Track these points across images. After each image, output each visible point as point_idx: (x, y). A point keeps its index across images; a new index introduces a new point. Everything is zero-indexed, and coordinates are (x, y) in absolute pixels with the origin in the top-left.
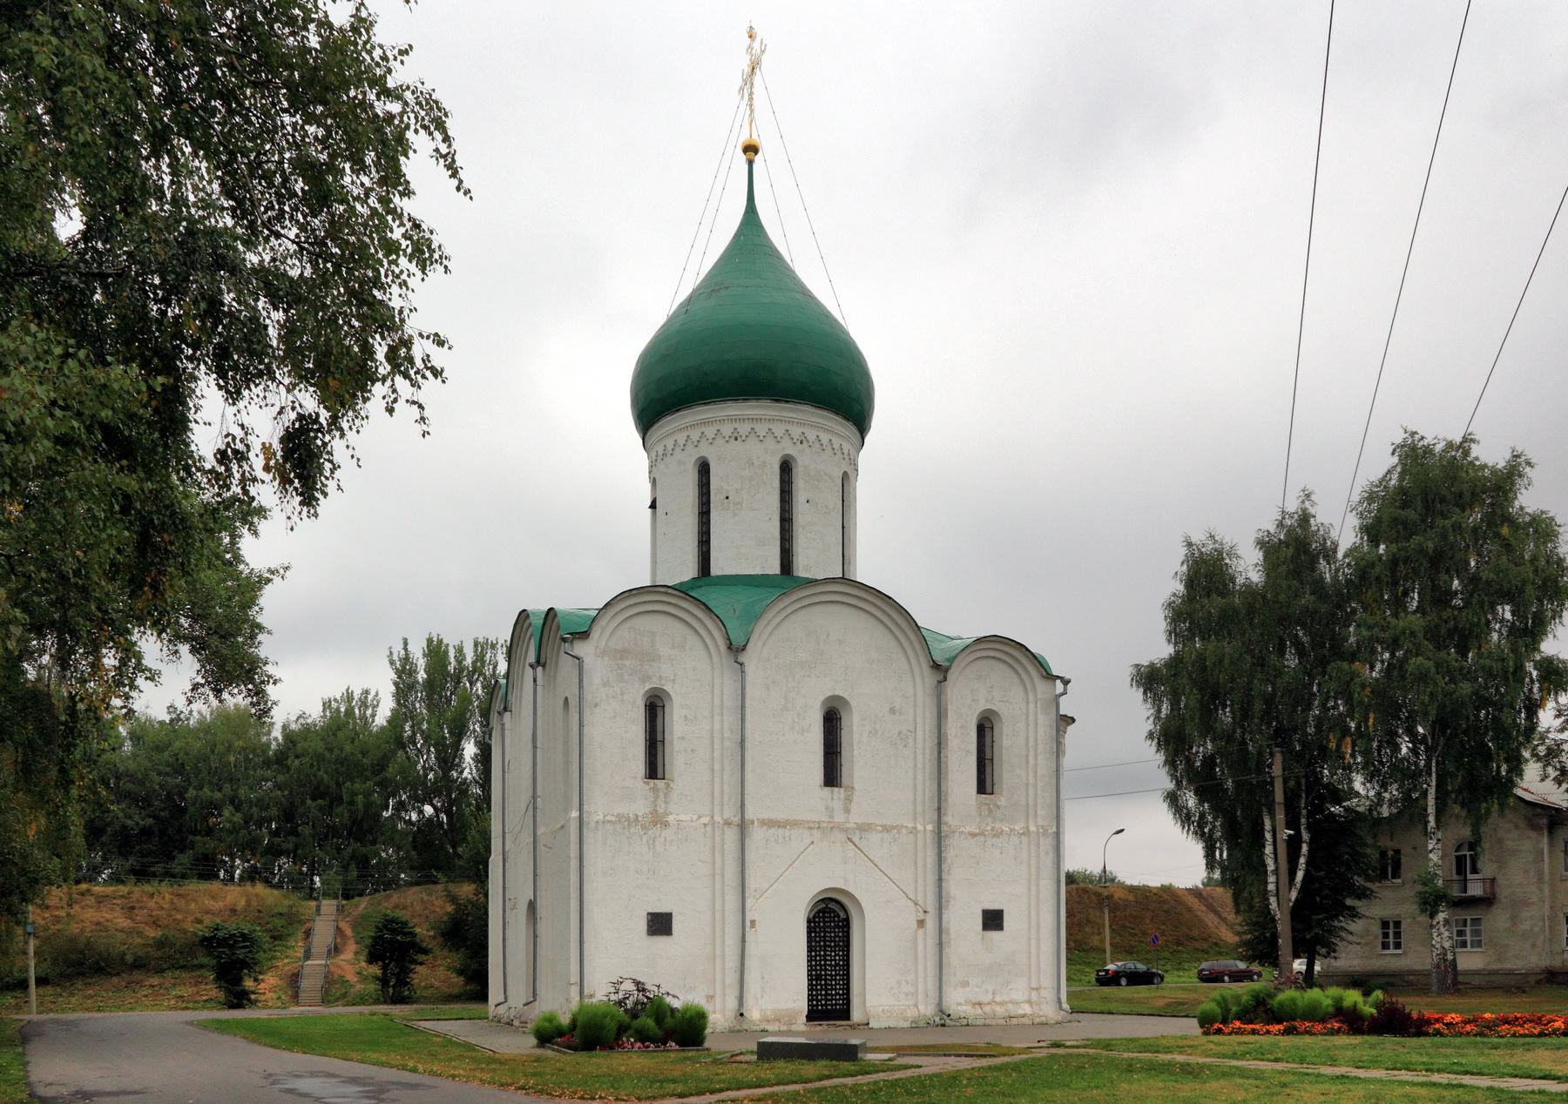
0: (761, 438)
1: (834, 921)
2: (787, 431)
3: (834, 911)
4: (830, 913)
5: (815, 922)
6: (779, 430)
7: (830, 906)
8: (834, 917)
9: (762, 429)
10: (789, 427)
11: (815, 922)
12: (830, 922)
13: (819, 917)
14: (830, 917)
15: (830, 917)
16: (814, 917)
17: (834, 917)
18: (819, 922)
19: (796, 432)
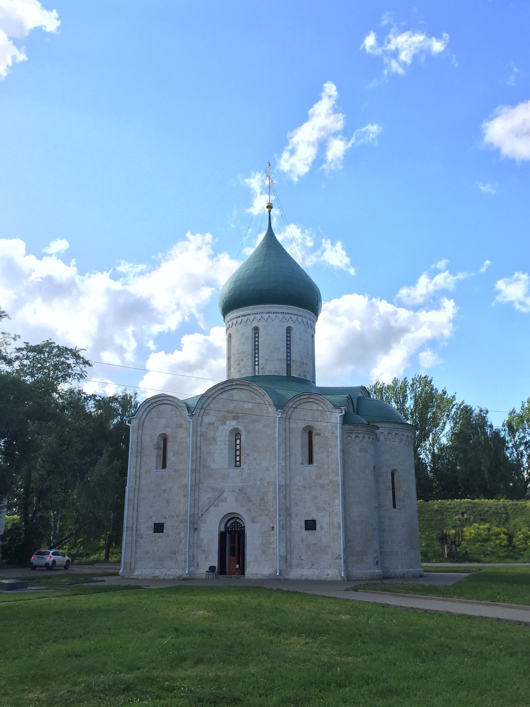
0: (294, 321)
1: (239, 528)
2: (291, 317)
3: (239, 523)
4: (237, 524)
5: (230, 528)
6: (251, 317)
7: (237, 521)
8: (239, 526)
9: (245, 319)
10: (255, 316)
11: (230, 528)
12: (237, 528)
13: (232, 526)
14: (237, 526)
15: (237, 526)
16: (230, 526)
17: (240, 525)
18: (232, 528)
19: (258, 317)
